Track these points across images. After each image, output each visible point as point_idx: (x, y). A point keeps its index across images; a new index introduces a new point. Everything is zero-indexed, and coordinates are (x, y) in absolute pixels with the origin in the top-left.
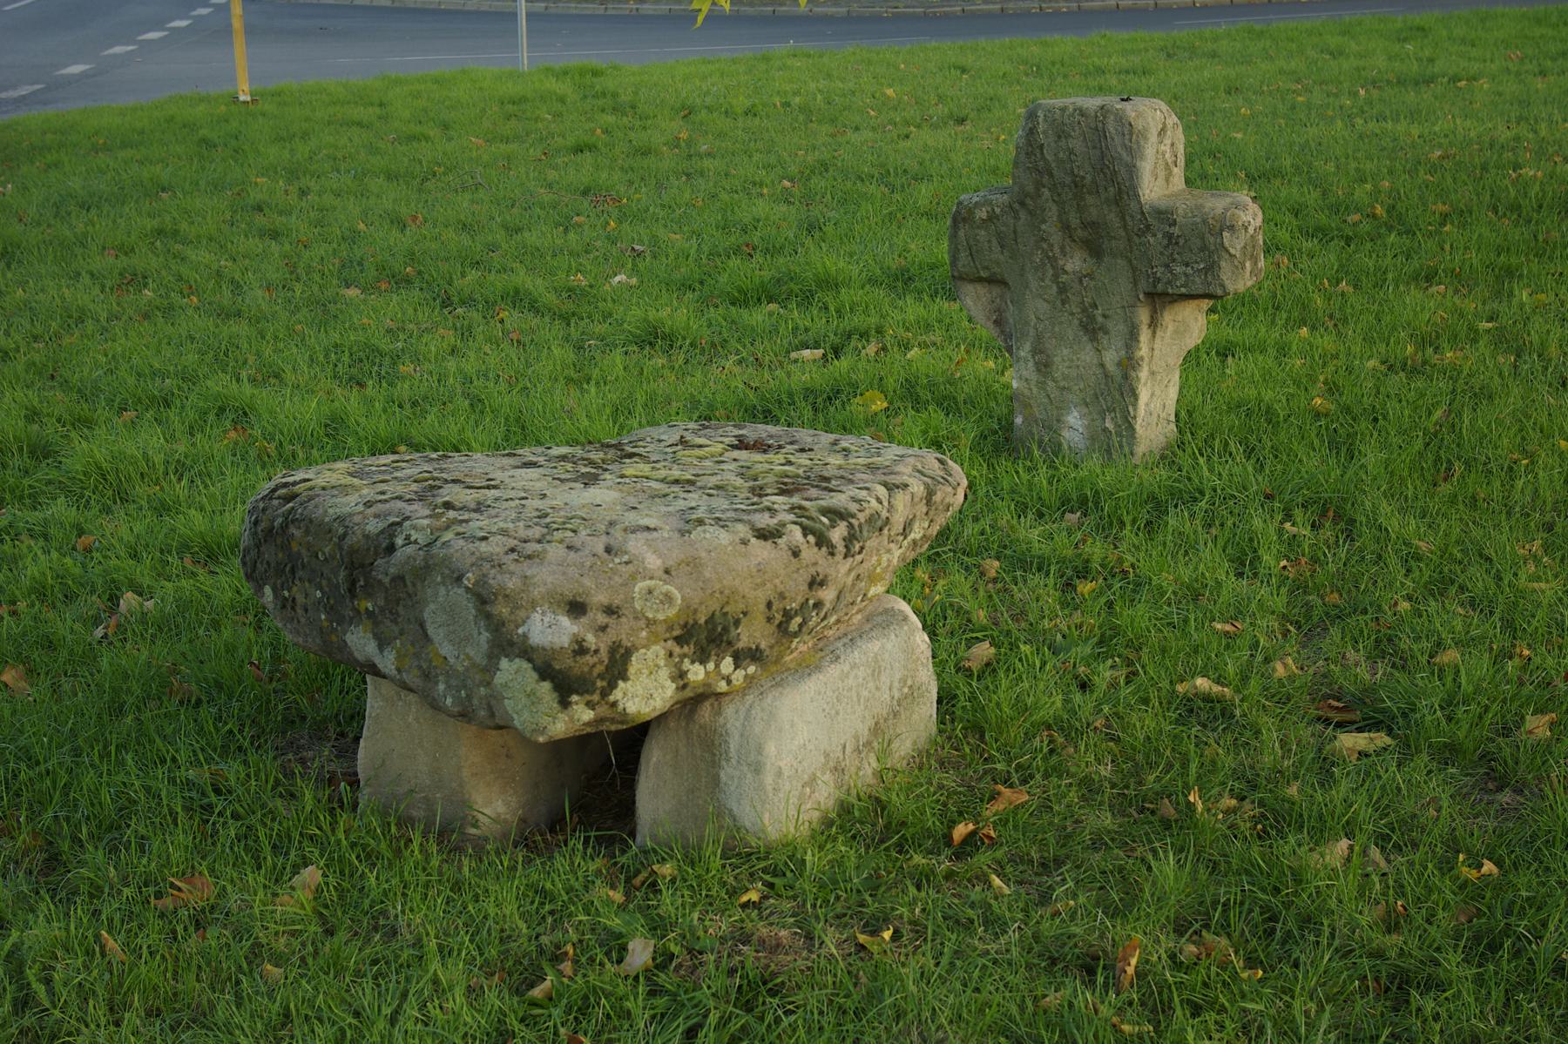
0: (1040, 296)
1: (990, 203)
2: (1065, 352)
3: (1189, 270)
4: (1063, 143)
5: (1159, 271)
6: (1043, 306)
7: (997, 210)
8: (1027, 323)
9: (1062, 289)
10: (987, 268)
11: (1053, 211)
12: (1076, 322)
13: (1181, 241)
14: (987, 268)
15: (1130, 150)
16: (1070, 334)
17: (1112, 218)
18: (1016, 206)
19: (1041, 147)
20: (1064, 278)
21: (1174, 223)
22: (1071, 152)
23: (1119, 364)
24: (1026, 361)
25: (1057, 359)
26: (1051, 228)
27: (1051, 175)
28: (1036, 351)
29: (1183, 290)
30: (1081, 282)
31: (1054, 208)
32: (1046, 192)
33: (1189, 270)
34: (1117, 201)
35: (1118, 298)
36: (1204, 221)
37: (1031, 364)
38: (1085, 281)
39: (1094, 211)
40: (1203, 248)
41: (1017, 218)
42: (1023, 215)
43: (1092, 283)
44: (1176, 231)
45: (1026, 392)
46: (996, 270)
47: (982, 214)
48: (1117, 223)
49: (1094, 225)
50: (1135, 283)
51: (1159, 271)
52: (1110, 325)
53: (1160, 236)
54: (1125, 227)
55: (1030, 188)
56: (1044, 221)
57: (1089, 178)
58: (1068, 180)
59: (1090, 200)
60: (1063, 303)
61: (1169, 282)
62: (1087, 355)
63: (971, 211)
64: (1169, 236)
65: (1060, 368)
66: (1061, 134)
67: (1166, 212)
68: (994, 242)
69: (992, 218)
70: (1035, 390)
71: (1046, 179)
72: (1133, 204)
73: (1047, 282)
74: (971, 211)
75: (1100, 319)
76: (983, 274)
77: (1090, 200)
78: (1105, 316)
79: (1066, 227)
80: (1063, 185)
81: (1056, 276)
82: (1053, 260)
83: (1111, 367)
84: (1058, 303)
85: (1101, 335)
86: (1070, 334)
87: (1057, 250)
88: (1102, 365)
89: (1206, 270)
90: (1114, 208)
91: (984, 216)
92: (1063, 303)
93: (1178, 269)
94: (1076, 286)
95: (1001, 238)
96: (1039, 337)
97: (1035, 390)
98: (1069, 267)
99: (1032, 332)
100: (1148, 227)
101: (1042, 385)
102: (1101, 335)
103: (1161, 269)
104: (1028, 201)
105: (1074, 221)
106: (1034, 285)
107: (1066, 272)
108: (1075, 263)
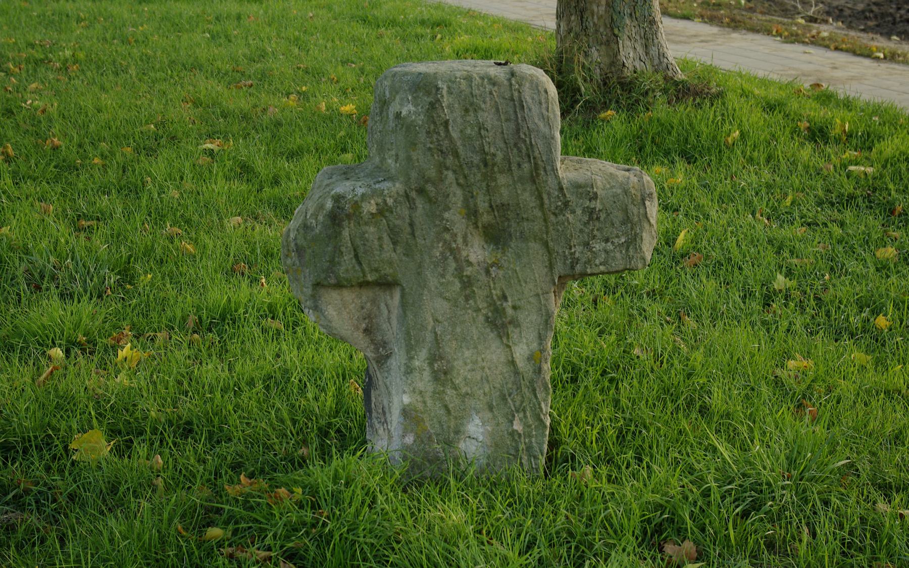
0: (441, 295)
1: (381, 193)
2: (467, 353)
3: (609, 246)
4: (471, 118)
5: (578, 250)
6: (441, 306)
7: (390, 201)
8: (423, 327)
9: (467, 283)
10: (377, 270)
11: (457, 196)
12: (481, 318)
13: (603, 216)
14: (377, 270)
15: (866, 141)
16: (475, 333)
17: (527, 197)
18: (413, 194)
19: (446, 123)
20: (468, 271)
21: (595, 197)
22: (481, 127)
23: (530, 358)
24: (421, 370)
25: (458, 364)
26: (455, 217)
27: (456, 155)
28: (433, 359)
29: (602, 268)
30: (488, 272)
31: (459, 192)
32: (450, 175)
33: (609, 246)
34: (533, 178)
35: (531, 286)
36: (626, 192)
37: (427, 374)
38: (493, 270)
39: (505, 192)
40: (627, 220)
41: (412, 208)
42: (420, 203)
43: (501, 273)
44: (598, 205)
45: (420, 406)
46: (389, 271)
47: (370, 207)
48: (532, 202)
49: (504, 207)
50: (551, 267)
51: (578, 250)
52: (521, 316)
53: (579, 212)
54: (542, 205)
55: (432, 173)
56: (447, 208)
57: (500, 155)
58: (476, 159)
59: (502, 179)
60: (467, 298)
61: (589, 262)
62: (494, 354)
63: (356, 205)
64: (591, 212)
65: (462, 372)
66: (470, 107)
67: (586, 186)
68: (386, 239)
69: (383, 211)
70: (429, 402)
71: (450, 161)
72: (551, 181)
73: (449, 277)
74: (356, 205)
75: (510, 311)
76: (370, 278)
77: (502, 179)
78: (515, 308)
79: (472, 214)
80: (470, 165)
81: (459, 270)
82: (454, 252)
83: (521, 364)
84: (461, 300)
85: (511, 329)
86: (475, 333)
87: (460, 240)
88: (512, 362)
89: (628, 245)
90: (529, 187)
91: (373, 209)
92: (467, 298)
93: (598, 246)
94: (483, 277)
95: (394, 235)
96: (437, 340)
97: (429, 402)
98: (473, 258)
99: (429, 337)
100: (566, 204)
101: (438, 395)
102: (511, 329)
103: (579, 249)
104: (429, 188)
105: (482, 204)
106: (433, 282)
107: (470, 264)
108: (477, 252)
